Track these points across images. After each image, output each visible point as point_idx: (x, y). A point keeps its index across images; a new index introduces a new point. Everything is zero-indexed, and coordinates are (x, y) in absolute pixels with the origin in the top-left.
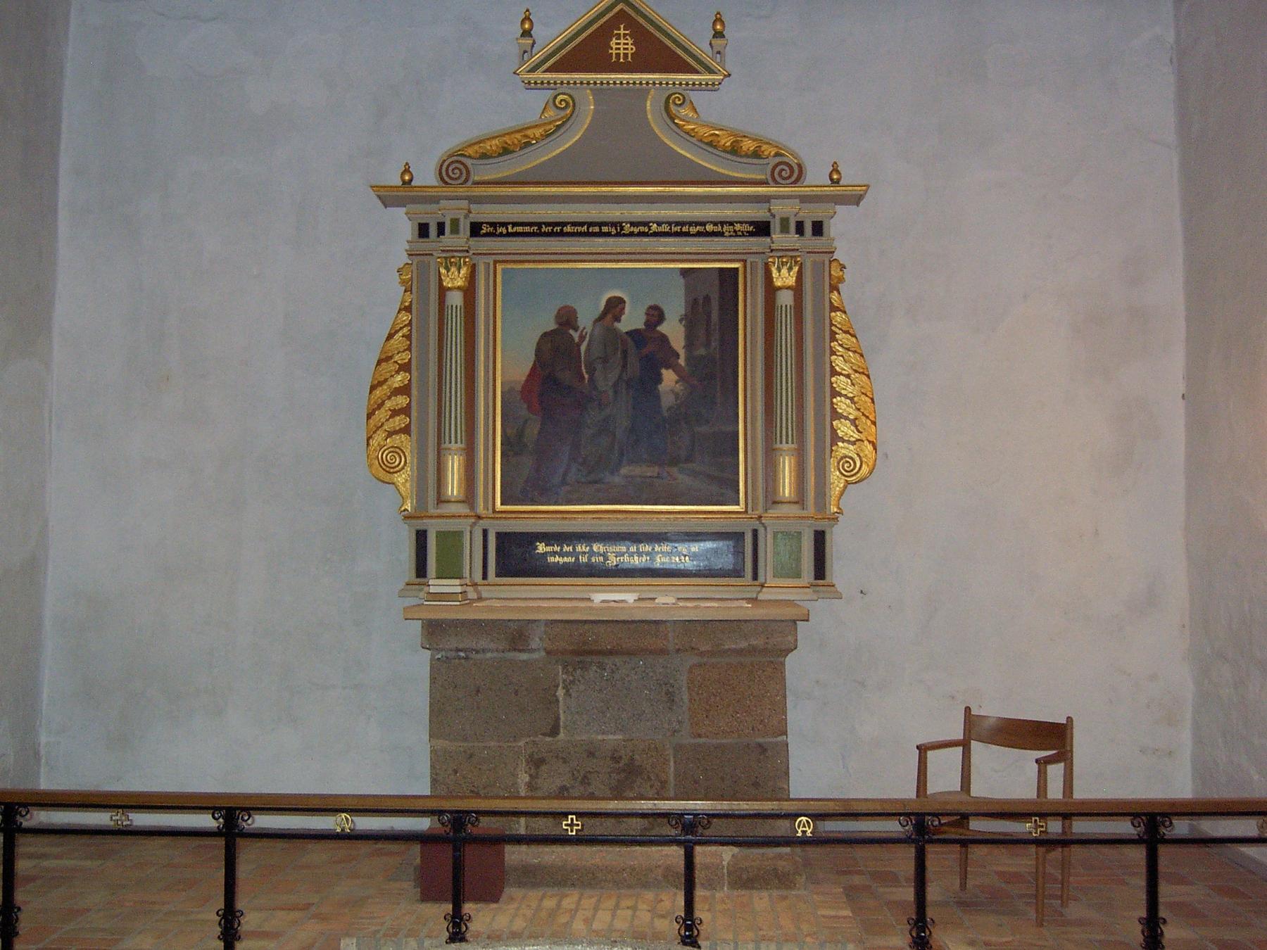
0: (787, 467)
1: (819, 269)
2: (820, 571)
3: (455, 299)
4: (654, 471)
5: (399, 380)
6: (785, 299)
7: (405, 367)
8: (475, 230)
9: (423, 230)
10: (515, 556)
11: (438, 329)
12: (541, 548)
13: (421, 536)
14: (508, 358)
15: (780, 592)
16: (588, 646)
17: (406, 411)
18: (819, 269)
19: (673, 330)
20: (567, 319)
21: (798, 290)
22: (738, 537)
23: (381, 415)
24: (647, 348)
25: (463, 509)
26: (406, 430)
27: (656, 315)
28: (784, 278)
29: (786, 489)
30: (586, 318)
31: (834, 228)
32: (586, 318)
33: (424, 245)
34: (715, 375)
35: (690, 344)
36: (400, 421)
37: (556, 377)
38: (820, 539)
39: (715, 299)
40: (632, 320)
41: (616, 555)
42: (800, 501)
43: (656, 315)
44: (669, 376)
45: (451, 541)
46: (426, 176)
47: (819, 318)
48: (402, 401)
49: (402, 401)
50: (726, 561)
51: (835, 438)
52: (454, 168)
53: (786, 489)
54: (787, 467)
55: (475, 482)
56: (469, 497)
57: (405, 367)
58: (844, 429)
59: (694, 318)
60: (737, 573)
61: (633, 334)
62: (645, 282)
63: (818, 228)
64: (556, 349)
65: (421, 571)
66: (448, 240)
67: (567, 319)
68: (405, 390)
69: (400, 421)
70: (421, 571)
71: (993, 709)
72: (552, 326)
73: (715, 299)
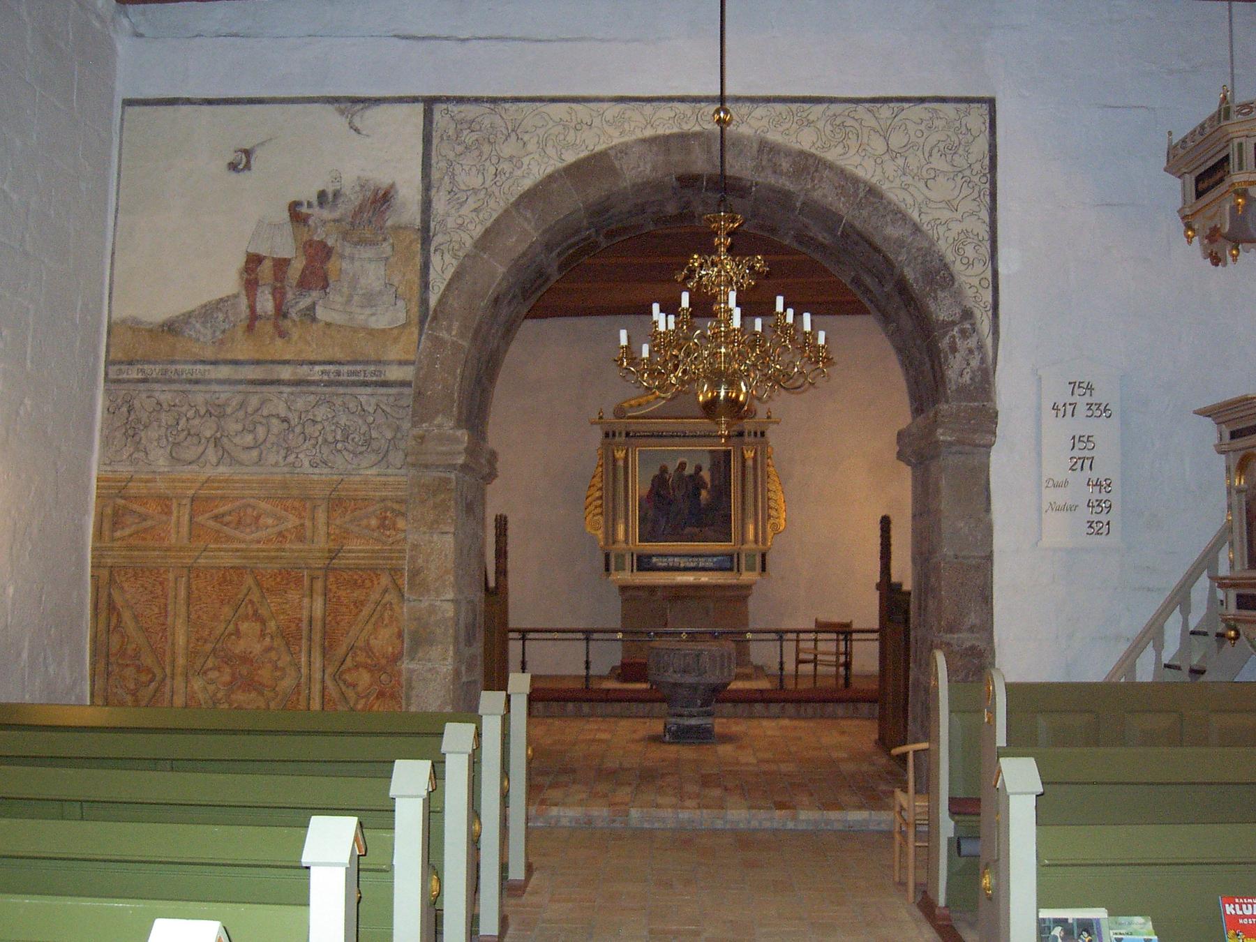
0: (751, 528)
1: (763, 452)
2: (764, 569)
3: (621, 463)
4: (697, 530)
5: (598, 494)
6: (750, 463)
7: (601, 489)
8: (627, 434)
9: (607, 435)
10: (644, 563)
11: (612, 472)
12: (654, 560)
13: (607, 556)
14: (639, 485)
15: (747, 577)
16: (678, 594)
17: (601, 506)
18: (763, 452)
19: (706, 475)
20: (664, 470)
21: (755, 459)
22: (731, 556)
23: (592, 508)
24: (695, 482)
25: (624, 545)
26: (601, 514)
27: (699, 469)
28: (749, 455)
29: (751, 536)
30: (672, 469)
31: (768, 434)
32: (672, 469)
33: (608, 440)
34: (722, 491)
35: (712, 480)
36: (598, 510)
37: (660, 492)
38: (764, 556)
39: (722, 462)
40: (689, 470)
41: (683, 563)
42: (756, 541)
43: (699, 469)
44: (704, 493)
45: (620, 556)
46: (609, 417)
47: (763, 470)
48: (599, 502)
49: (599, 502)
50: (728, 565)
51: (770, 517)
52: (620, 412)
53: (751, 536)
54: (751, 528)
55: (627, 534)
56: (626, 541)
57: (601, 489)
58: (773, 513)
59: (714, 467)
60: (731, 569)
61: (691, 476)
62: (693, 456)
63: (763, 434)
64: (660, 481)
65: (607, 569)
66: (617, 439)
67: (664, 470)
68: (601, 498)
69: (598, 510)
70: (607, 569)
71: (824, 617)
72: (657, 473)
73: (722, 462)
